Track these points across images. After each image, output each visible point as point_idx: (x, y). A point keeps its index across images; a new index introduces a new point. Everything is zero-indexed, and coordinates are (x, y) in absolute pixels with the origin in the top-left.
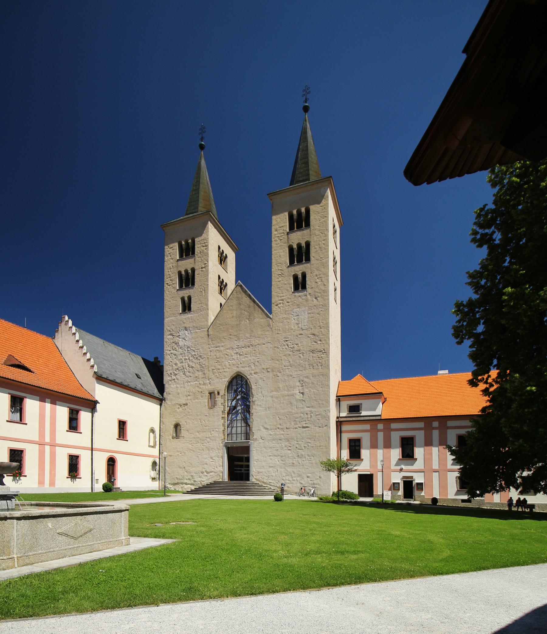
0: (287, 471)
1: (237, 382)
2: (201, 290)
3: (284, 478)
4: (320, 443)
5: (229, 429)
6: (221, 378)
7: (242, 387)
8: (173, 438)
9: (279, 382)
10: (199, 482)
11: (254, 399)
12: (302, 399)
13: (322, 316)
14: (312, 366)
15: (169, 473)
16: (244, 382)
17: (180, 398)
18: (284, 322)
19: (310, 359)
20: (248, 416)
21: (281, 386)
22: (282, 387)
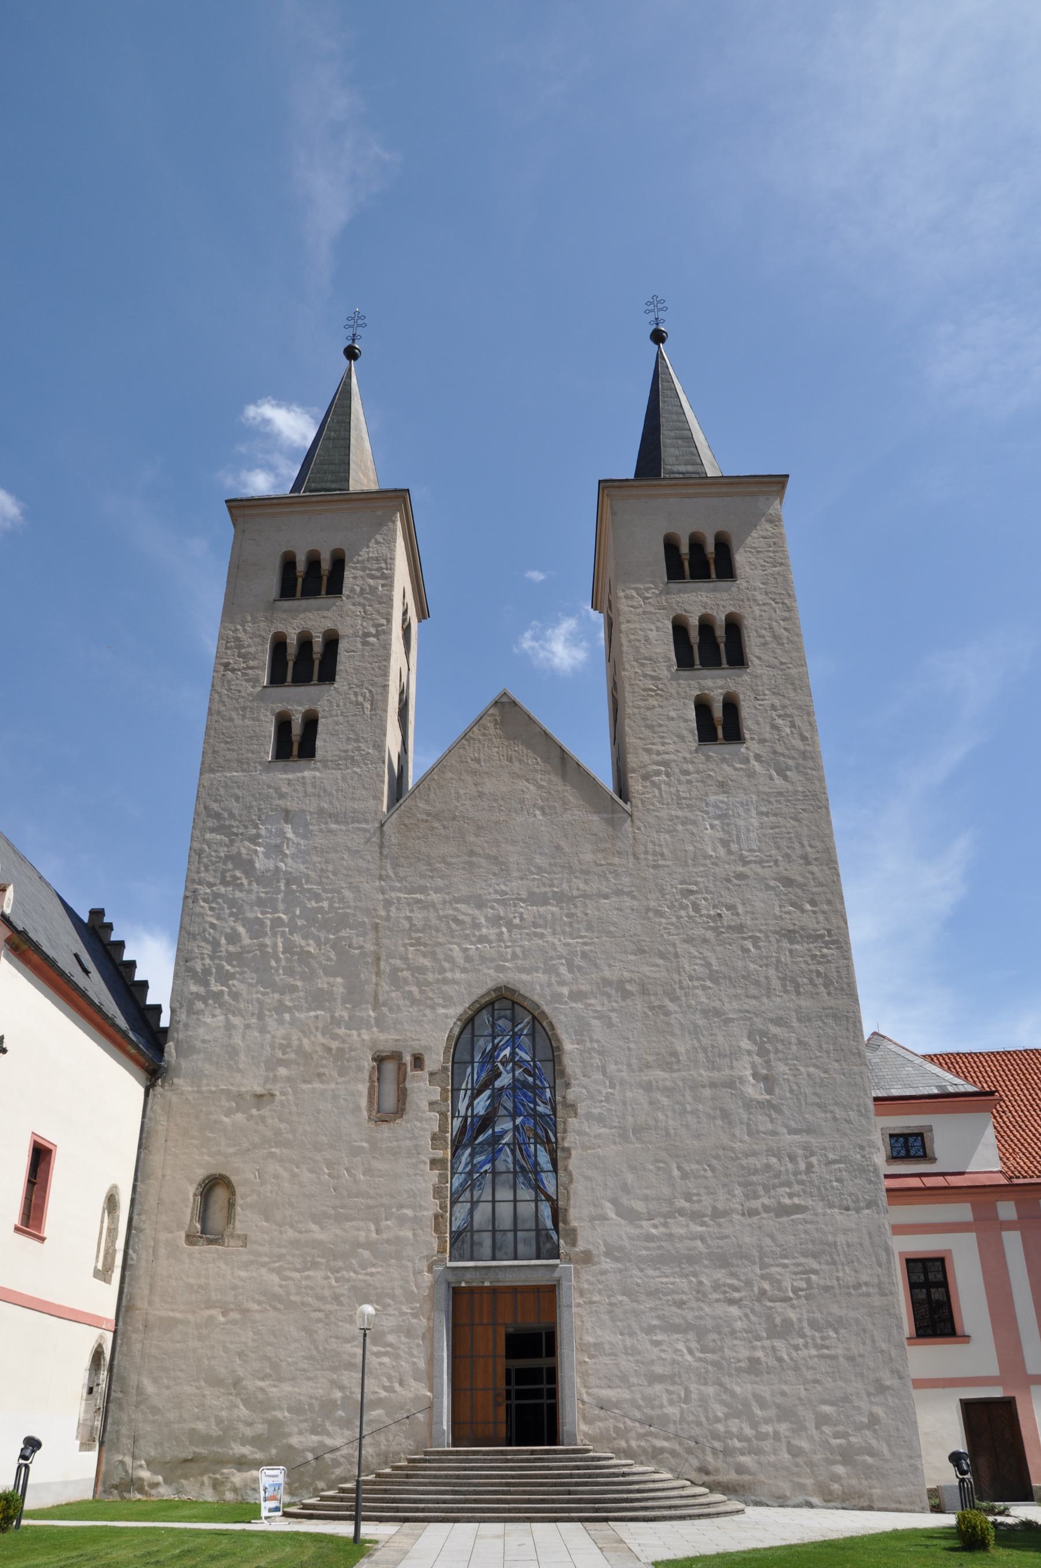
0: (733, 1394)
1: (493, 1025)
2: (360, 699)
3: (720, 1427)
4: (856, 1271)
5: (461, 1211)
6: (429, 1002)
7: (514, 1041)
8: (191, 1239)
9: (673, 1034)
10: (310, 1456)
11: (572, 1094)
12: (768, 1101)
13: (808, 826)
14: (791, 983)
15: (155, 1410)
16: (524, 1025)
17: (239, 1070)
18: (676, 831)
19: (783, 959)
20: (544, 1158)
21: (681, 1048)
22: (687, 1051)
